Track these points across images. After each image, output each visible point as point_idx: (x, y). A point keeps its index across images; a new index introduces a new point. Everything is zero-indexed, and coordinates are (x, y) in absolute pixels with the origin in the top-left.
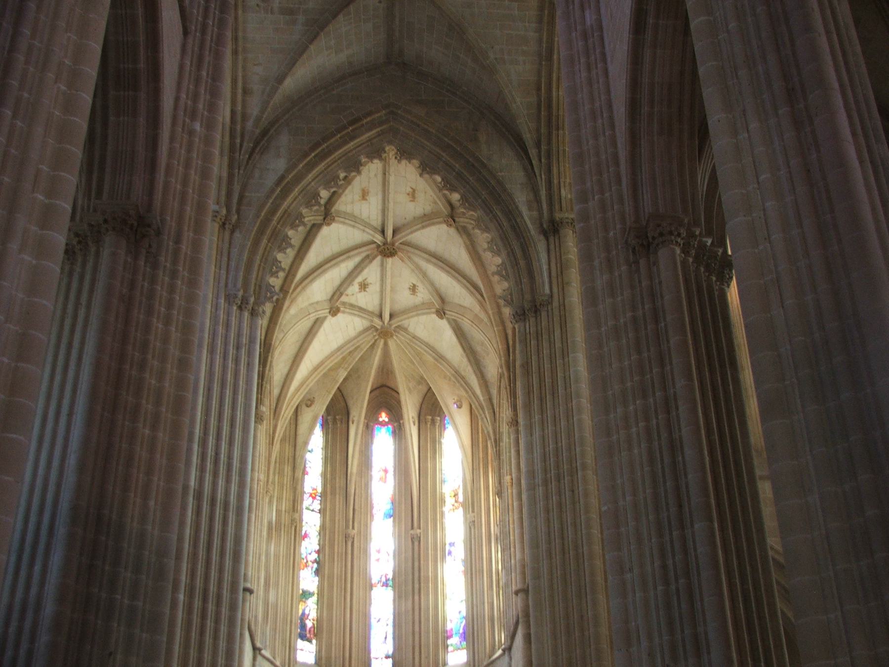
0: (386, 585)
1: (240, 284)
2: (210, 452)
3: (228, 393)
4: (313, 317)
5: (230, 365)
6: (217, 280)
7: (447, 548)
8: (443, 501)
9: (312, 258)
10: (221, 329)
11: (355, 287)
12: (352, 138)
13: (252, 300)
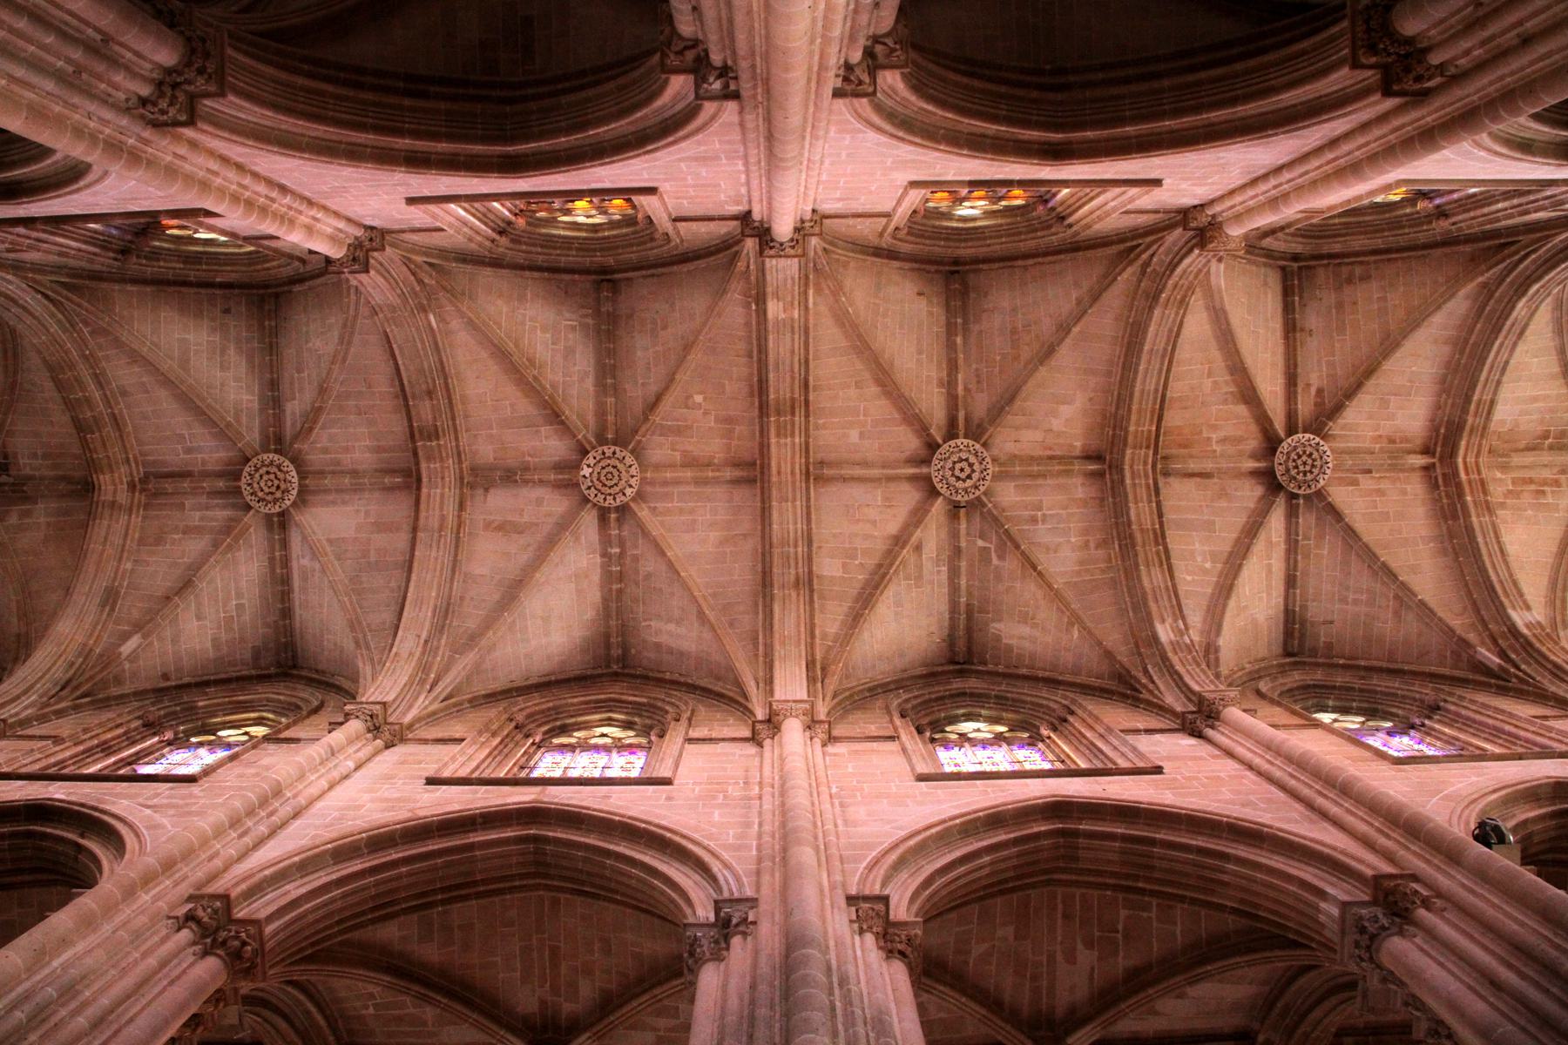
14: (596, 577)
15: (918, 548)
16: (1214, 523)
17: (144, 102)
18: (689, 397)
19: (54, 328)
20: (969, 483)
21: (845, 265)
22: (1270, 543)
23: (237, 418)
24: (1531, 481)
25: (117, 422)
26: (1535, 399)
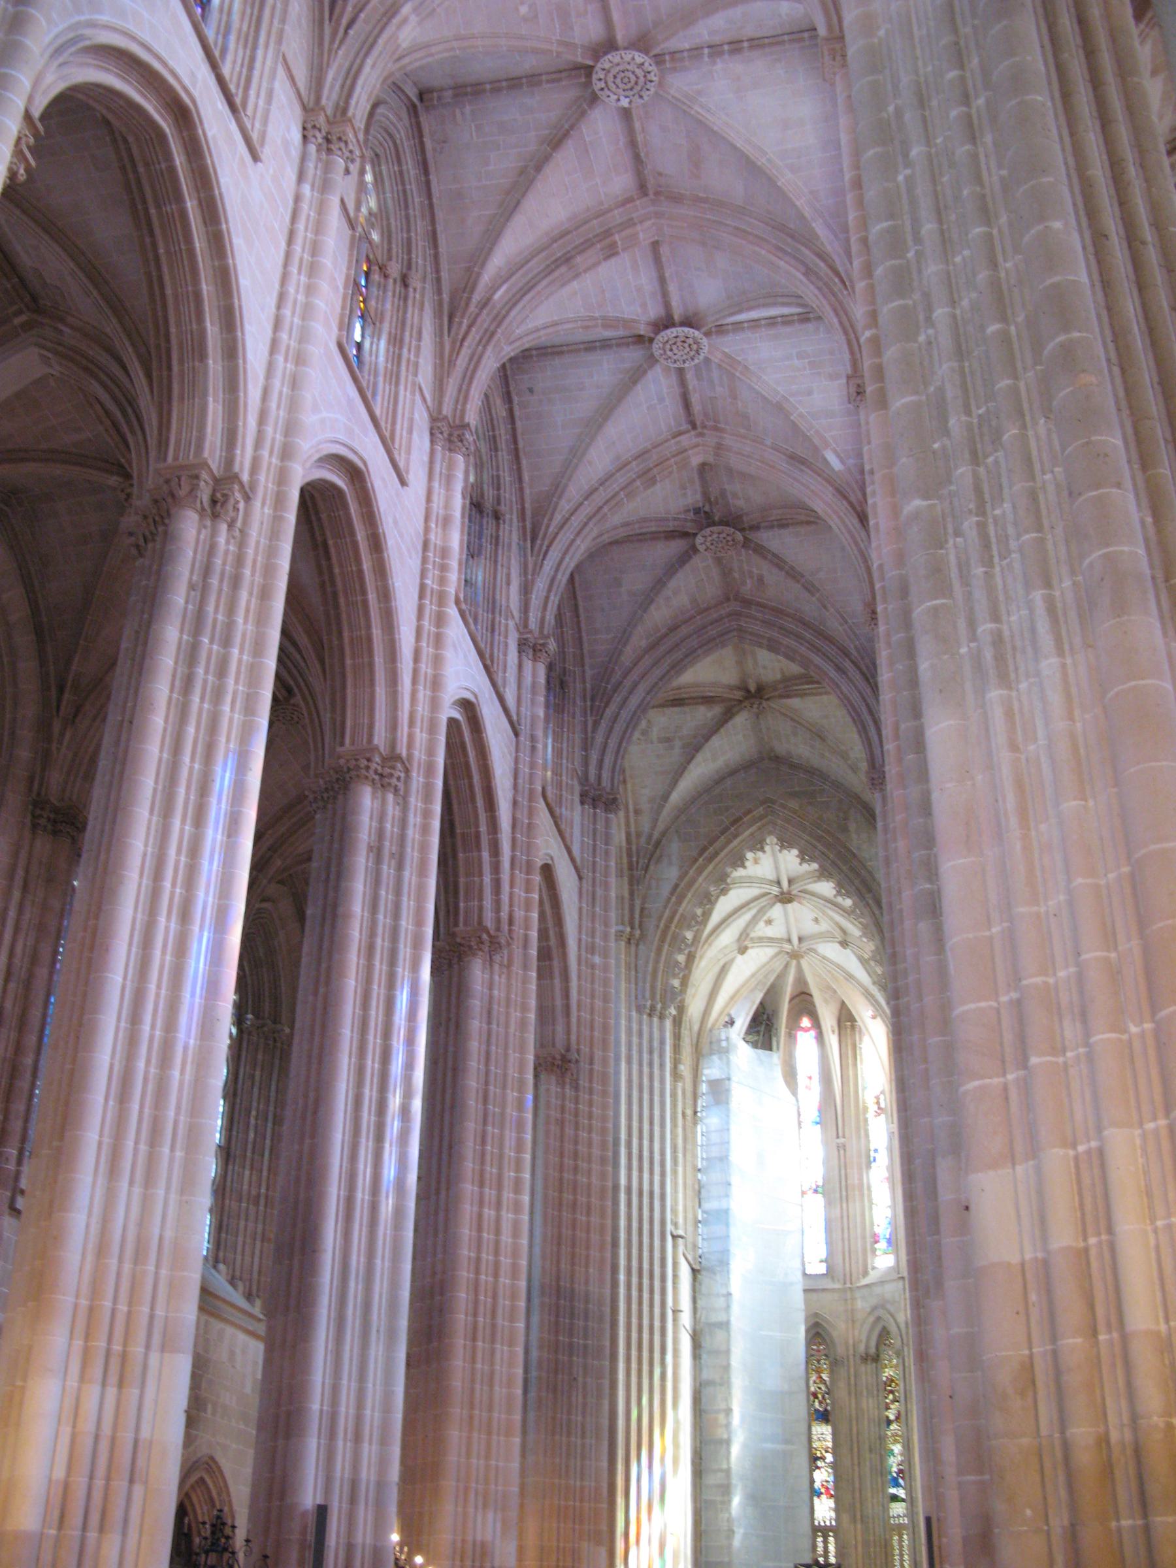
0: (816, 1191)
1: (648, 994)
2: (635, 1151)
3: (646, 1096)
4: (721, 963)
5: (646, 1069)
6: (628, 995)
7: (872, 1154)
8: (866, 1109)
9: (715, 918)
10: (635, 1040)
11: (762, 924)
12: (736, 836)
13: (659, 1006)
17: (396, 790)
18: (525, 19)
25: (641, 455)
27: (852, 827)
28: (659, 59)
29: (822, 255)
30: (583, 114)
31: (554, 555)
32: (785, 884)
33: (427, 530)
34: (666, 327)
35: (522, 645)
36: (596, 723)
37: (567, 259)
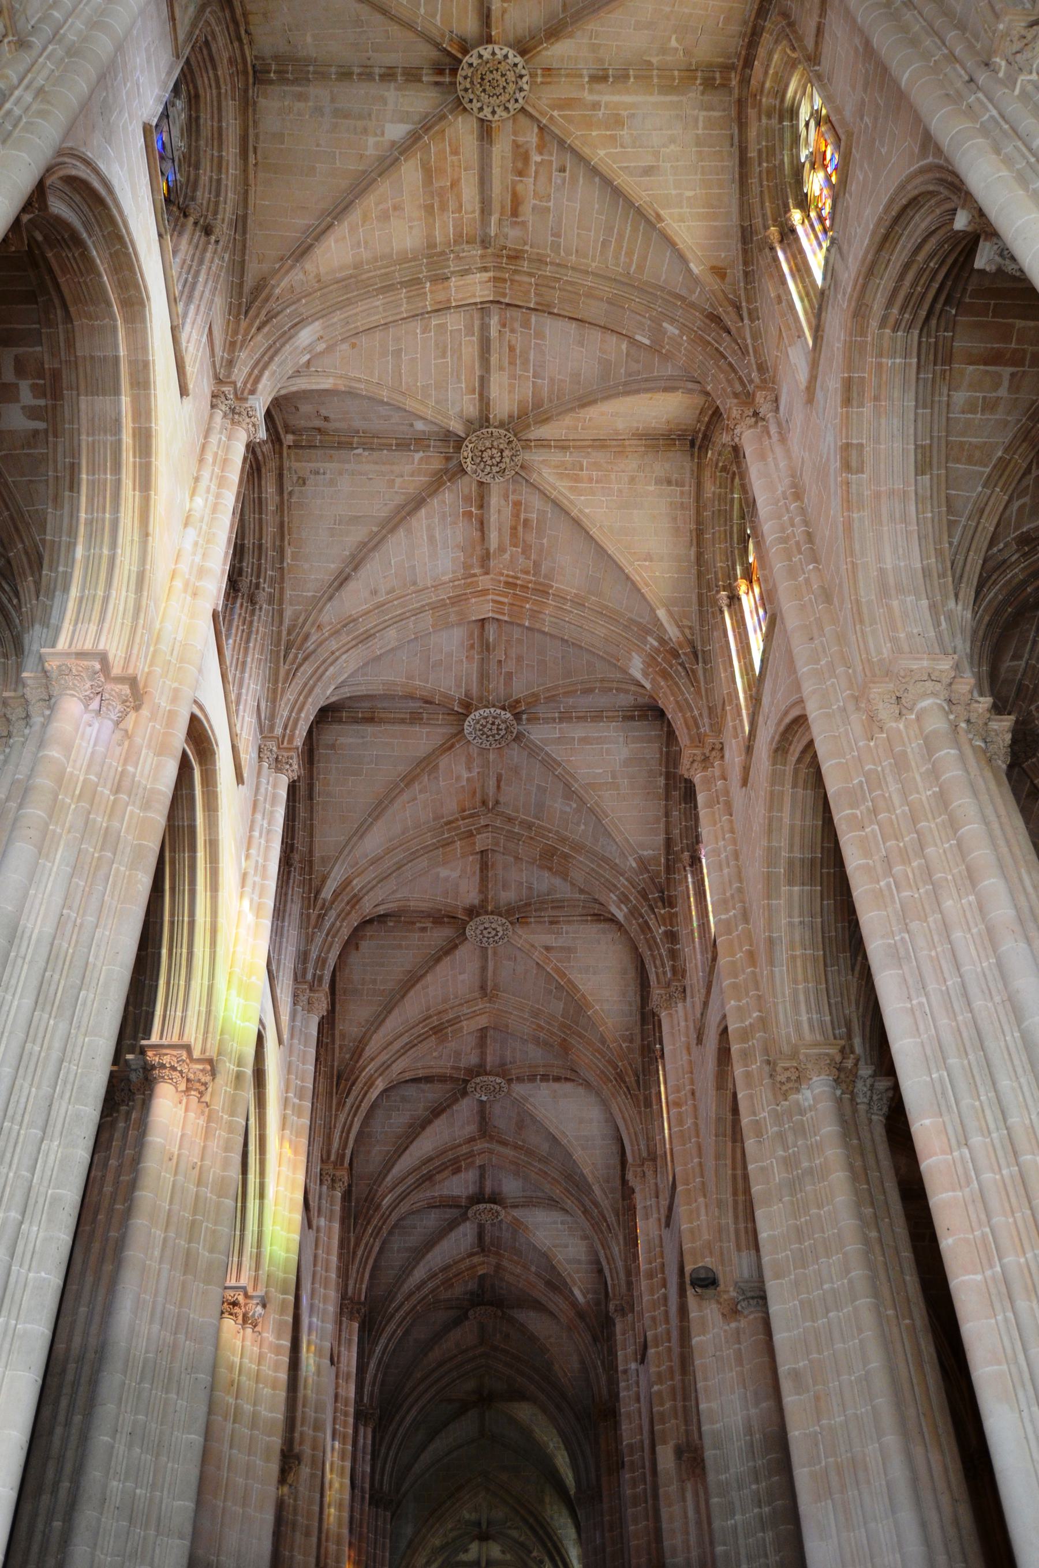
14: (556, 1086)
15: (548, 949)
16: (538, 786)
19: (392, 1326)
20: (499, 929)
21: (343, 1036)
22: (559, 740)
23: (445, 1220)
24: (514, 528)
25: (446, 1268)
26: (431, 539)
27: (547, 1500)
28: (510, 1081)
29: (596, 1204)
30: (456, 1100)
31: (383, 1341)
32: (484, 1526)
33: (337, 1388)
34: (478, 1202)
35: (359, 1415)
36: (382, 1439)
37: (429, 1178)
